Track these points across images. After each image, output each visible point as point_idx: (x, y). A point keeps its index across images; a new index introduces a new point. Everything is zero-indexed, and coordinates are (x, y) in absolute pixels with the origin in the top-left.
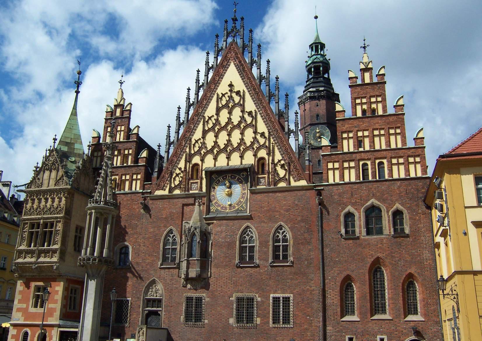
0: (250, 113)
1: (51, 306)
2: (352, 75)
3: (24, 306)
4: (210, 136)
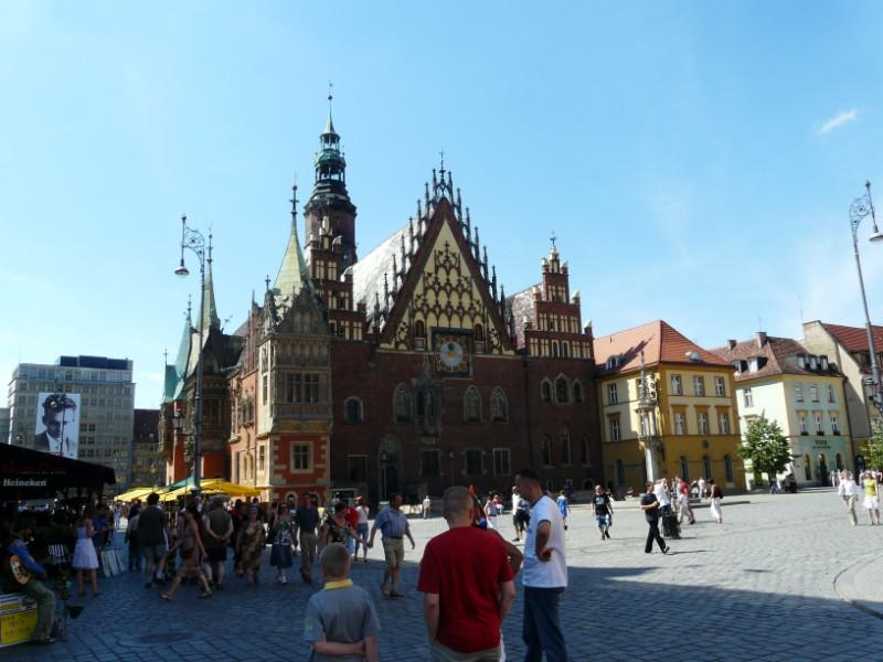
0: (466, 279)
1: (318, 466)
3: (284, 467)
4: (431, 294)
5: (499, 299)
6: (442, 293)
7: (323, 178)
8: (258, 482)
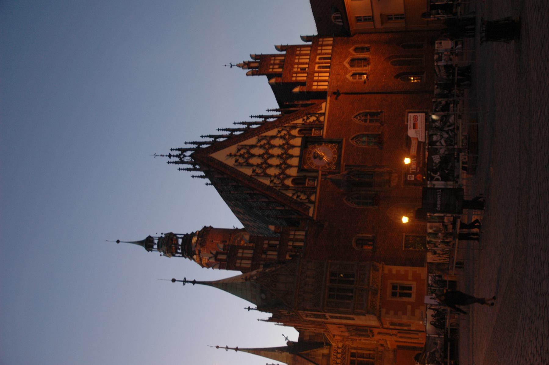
0: (259, 141)
1: (410, 278)
2: (250, 73)
3: (409, 307)
5: (278, 113)
6: (270, 161)
7: (180, 251)
8: (421, 330)
